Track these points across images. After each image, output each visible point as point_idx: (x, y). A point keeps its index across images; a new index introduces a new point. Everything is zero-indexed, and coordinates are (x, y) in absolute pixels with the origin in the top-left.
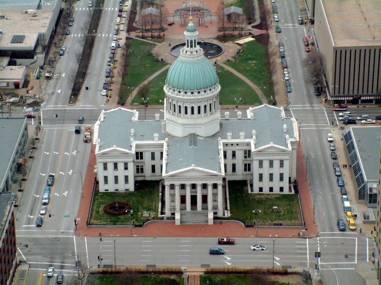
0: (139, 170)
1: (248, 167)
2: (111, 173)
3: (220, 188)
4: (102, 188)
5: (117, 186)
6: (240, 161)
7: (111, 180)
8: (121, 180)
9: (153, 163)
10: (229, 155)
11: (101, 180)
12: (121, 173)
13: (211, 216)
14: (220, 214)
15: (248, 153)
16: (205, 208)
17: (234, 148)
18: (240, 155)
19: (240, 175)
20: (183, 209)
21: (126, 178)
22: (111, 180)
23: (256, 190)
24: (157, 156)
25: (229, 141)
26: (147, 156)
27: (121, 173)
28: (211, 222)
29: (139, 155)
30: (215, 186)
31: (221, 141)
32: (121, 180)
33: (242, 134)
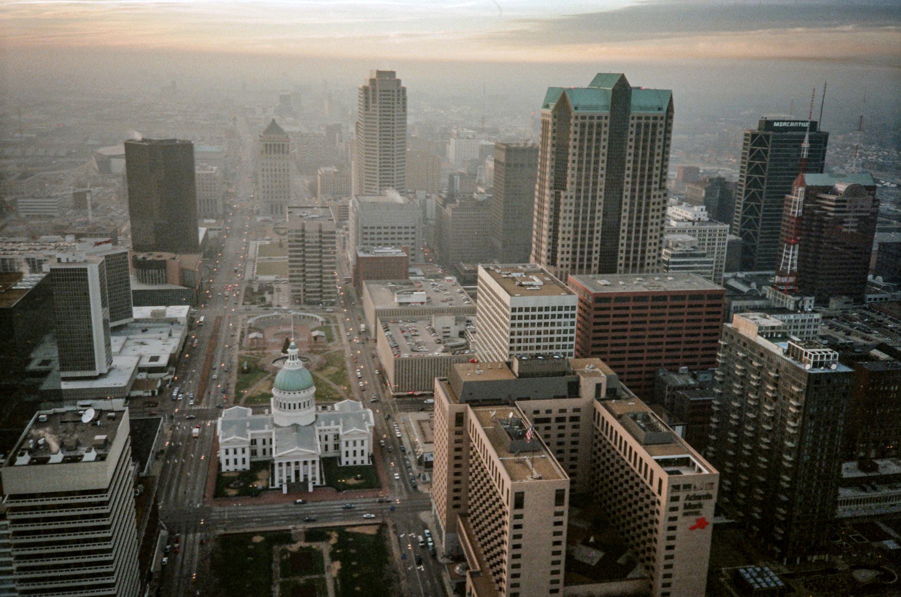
0: (254, 453)
1: (337, 447)
2: (231, 457)
4: (224, 468)
6: (331, 442)
7: (231, 462)
8: (240, 461)
9: (264, 447)
10: (323, 438)
11: (223, 462)
14: (318, 483)
15: (337, 437)
17: (326, 433)
19: (331, 453)
20: (289, 481)
22: (231, 462)
23: (344, 464)
24: (267, 442)
25: (323, 427)
26: (260, 442)
28: (311, 489)
29: (253, 442)
30: (313, 462)
31: (317, 428)
32: (240, 461)
33: (333, 422)
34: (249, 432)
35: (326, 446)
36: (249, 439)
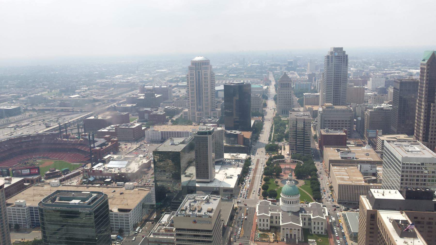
0: (272, 222)
1: (310, 224)
3: (300, 231)
5: (264, 228)
7: (262, 225)
8: (265, 225)
9: (276, 220)
10: (303, 219)
12: (265, 223)
13: (297, 241)
15: (310, 219)
16: (295, 238)
17: (305, 217)
18: (307, 219)
19: (307, 226)
21: (267, 225)
22: (262, 225)
24: (278, 218)
25: (303, 214)
26: (274, 218)
27: (265, 223)
29: (272, 217)
30: (299, 230)
32: (265, 225)
34: (270, 213)
35: (305, 223)
36: (270, 215)
